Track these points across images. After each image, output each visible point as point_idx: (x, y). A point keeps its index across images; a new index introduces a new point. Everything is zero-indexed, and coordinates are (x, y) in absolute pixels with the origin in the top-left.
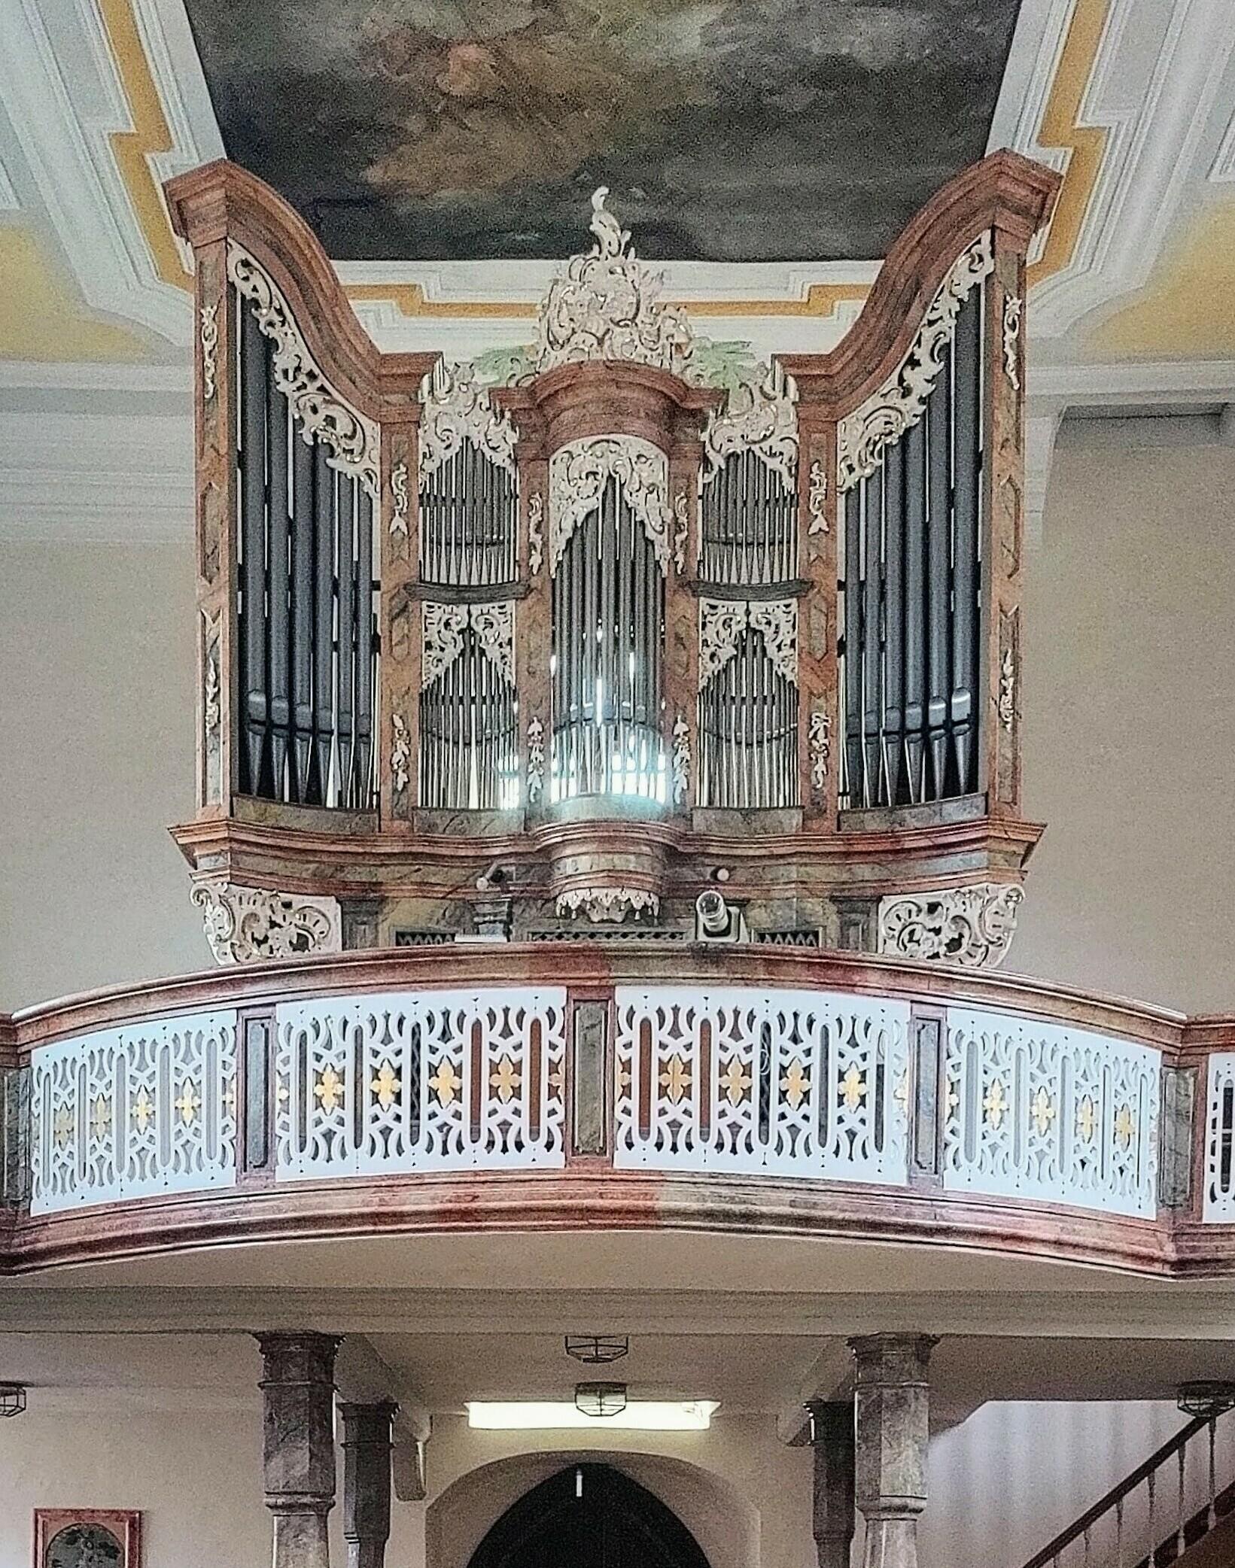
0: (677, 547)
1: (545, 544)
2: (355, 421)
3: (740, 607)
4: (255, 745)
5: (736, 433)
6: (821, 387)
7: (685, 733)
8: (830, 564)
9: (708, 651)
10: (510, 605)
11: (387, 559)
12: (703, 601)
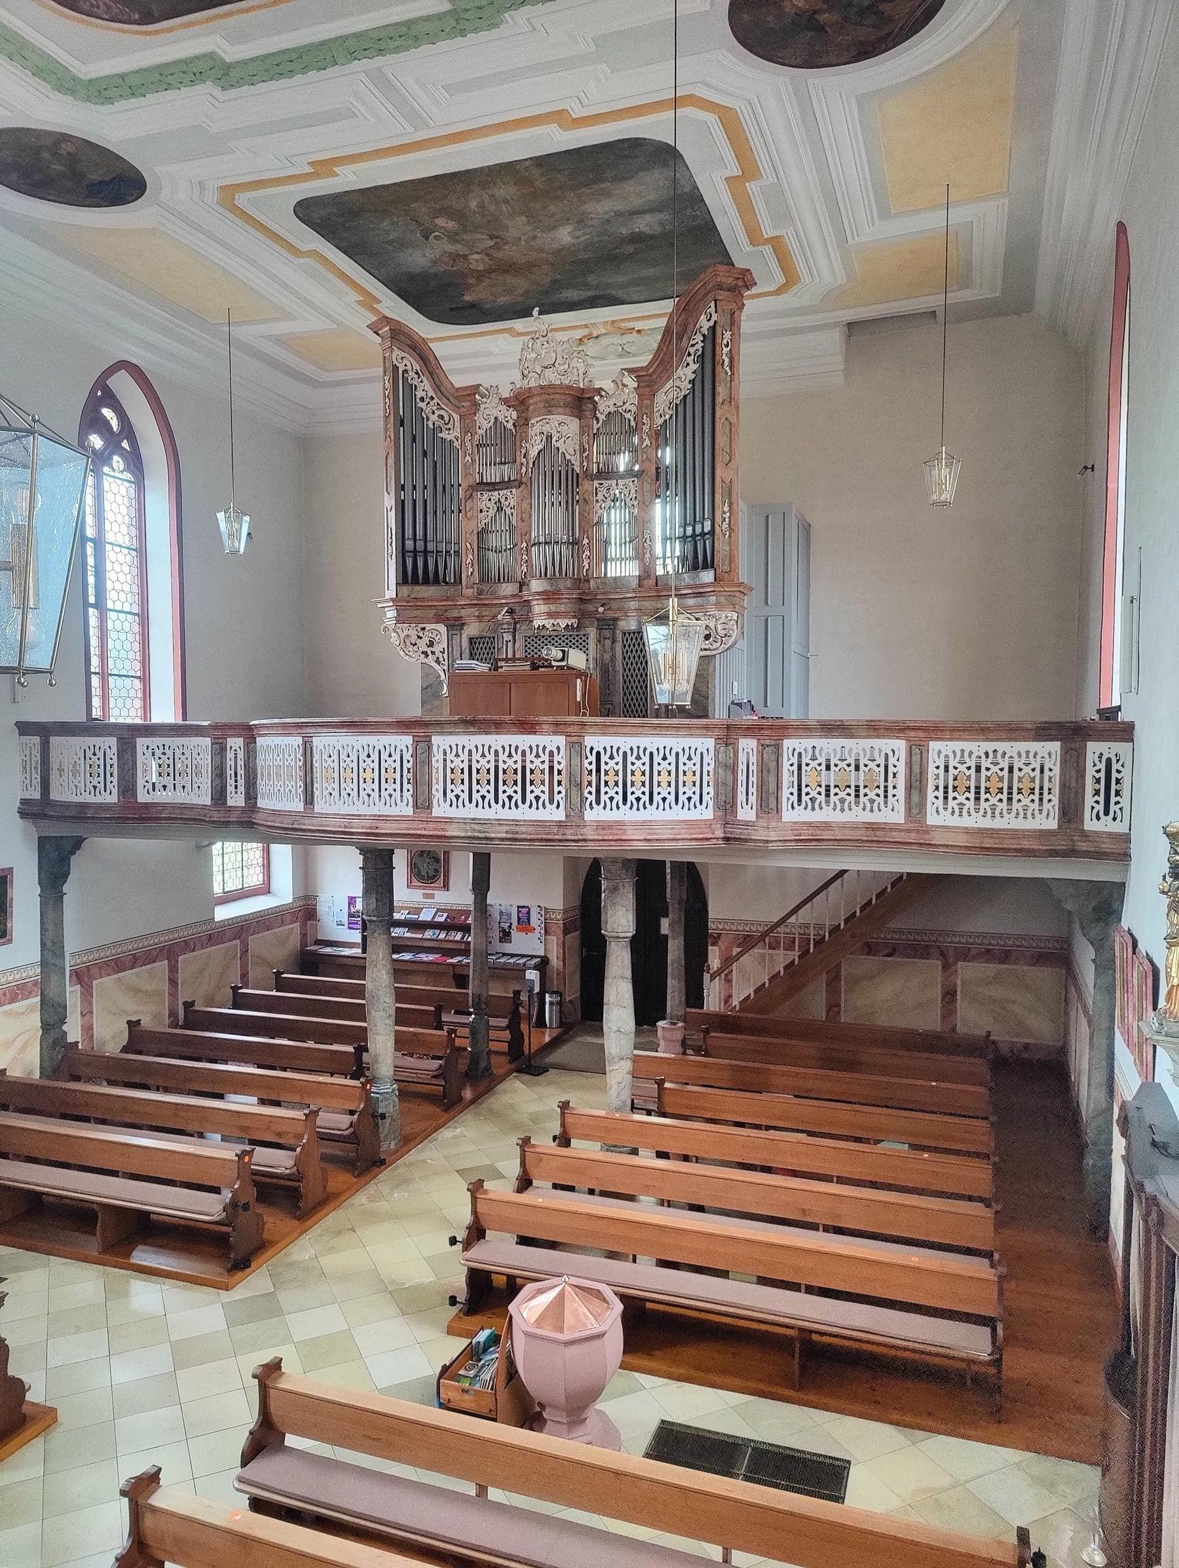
4: (409, 561)
5: (611, 403)
6: (648, 380)
12: (596, 483)
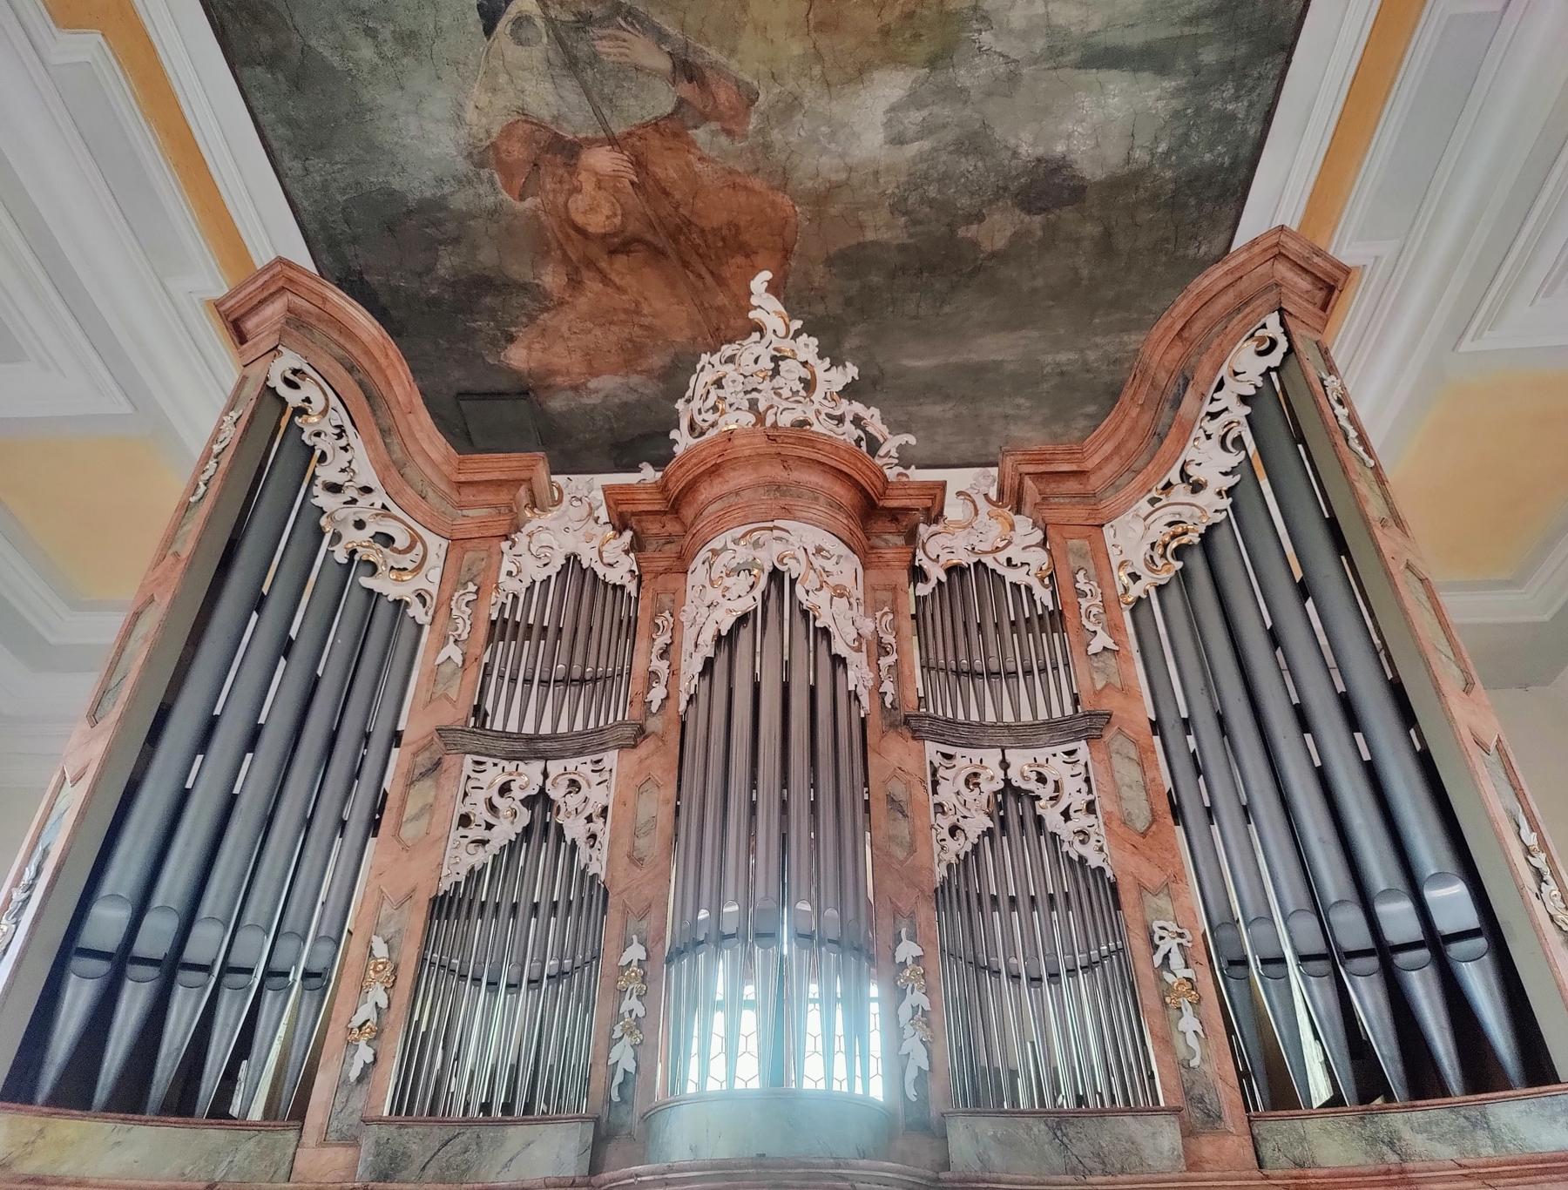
0: (883, 674)
1: (674, 673)
2: (415, 539)
3: (992, 757)
7: (917, 960)
8: (1126, 691)
9: (945, 822)
10: (611, 758)
11: (425, 696)
12: (932, 749)
